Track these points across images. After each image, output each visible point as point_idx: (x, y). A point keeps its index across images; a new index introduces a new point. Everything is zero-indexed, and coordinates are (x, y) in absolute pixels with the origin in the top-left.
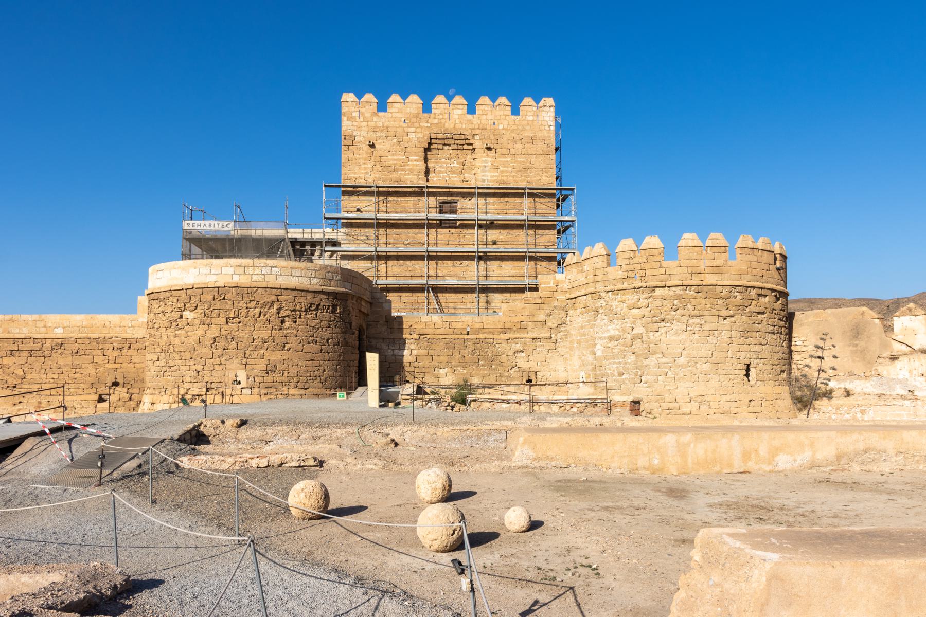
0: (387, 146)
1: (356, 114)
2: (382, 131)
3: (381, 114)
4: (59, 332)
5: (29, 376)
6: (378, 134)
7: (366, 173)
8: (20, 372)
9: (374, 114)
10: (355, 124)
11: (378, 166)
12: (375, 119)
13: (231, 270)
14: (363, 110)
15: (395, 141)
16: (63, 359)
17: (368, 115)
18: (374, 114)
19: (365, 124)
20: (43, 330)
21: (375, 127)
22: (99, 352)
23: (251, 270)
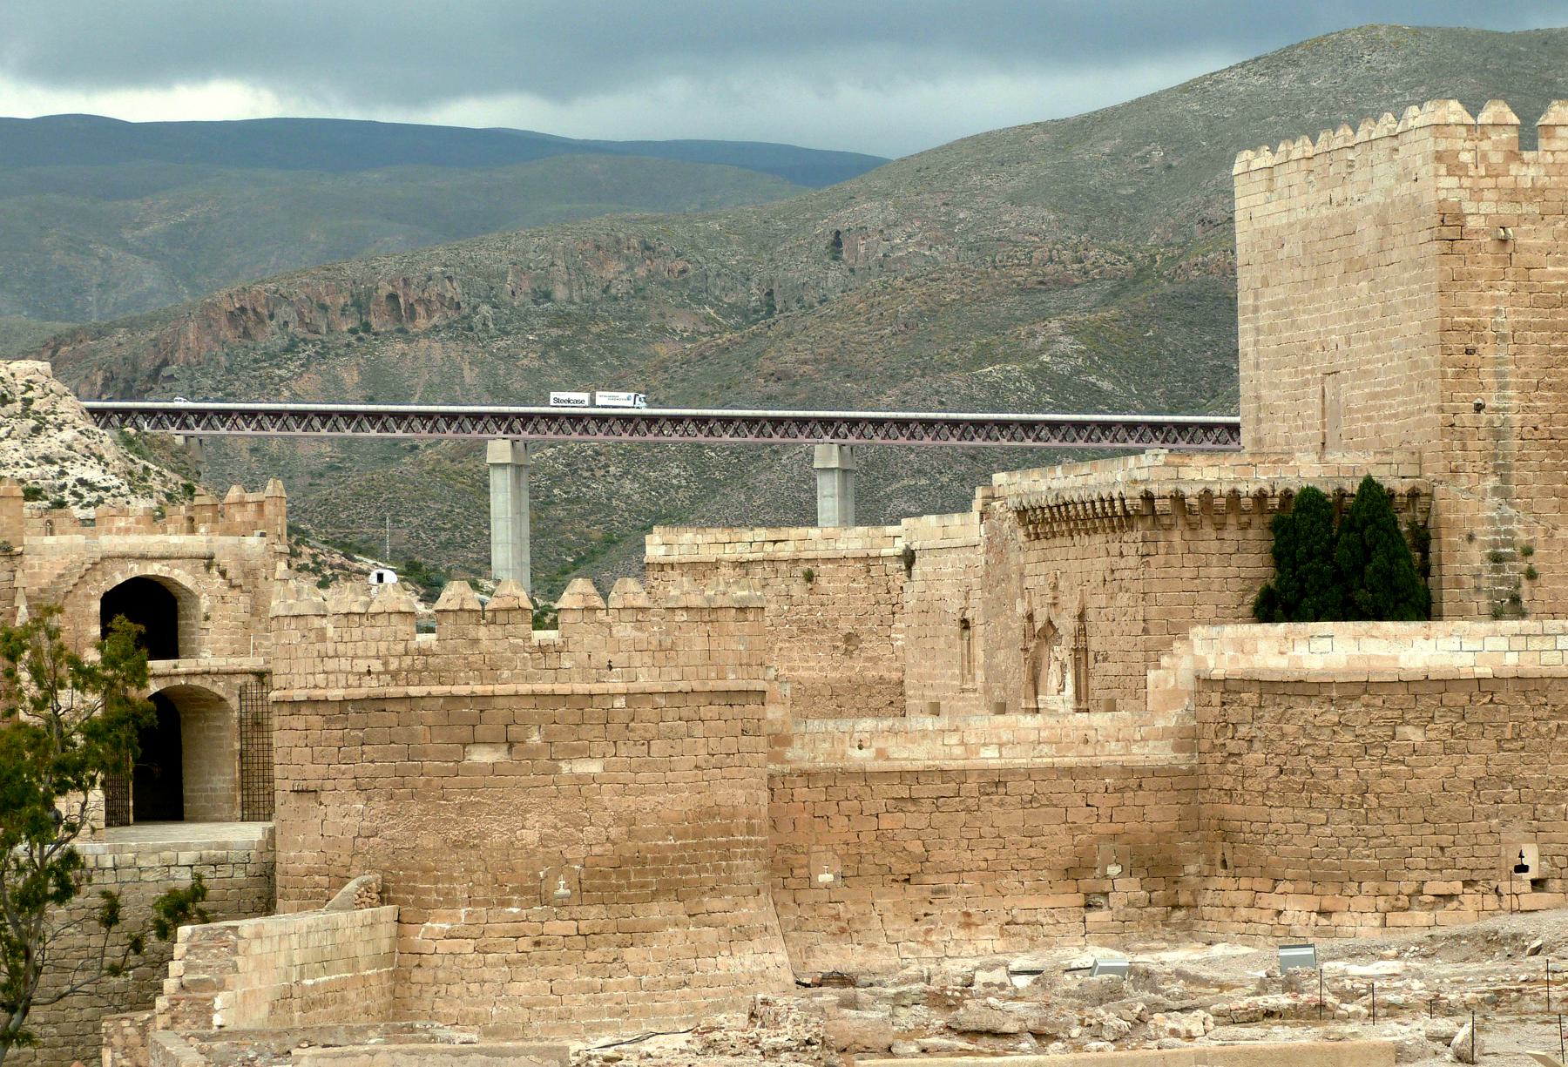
0: (1544, 239)
1: (1466, 157)
2: (1530, 200)
3: (1527, 155)
4: (990, 757)
5: (936, 856)
6: (1527, 208)
7: (1497, 312)
8: (916, 847)
9: (1513, 156)
10: (1467, 182)
11: (1523, 293)
12: (1514, 168)
13: (1502, 644)
14: (1485, 145)
15: (1561, 225)
16: (1003, 817)
17: (1496, 158)
18: (1513, 156)
19: (1490, 182)
20: (958, 751)
21: (1515, 190)
22: (1078, 799)
23: (1535, 644)
